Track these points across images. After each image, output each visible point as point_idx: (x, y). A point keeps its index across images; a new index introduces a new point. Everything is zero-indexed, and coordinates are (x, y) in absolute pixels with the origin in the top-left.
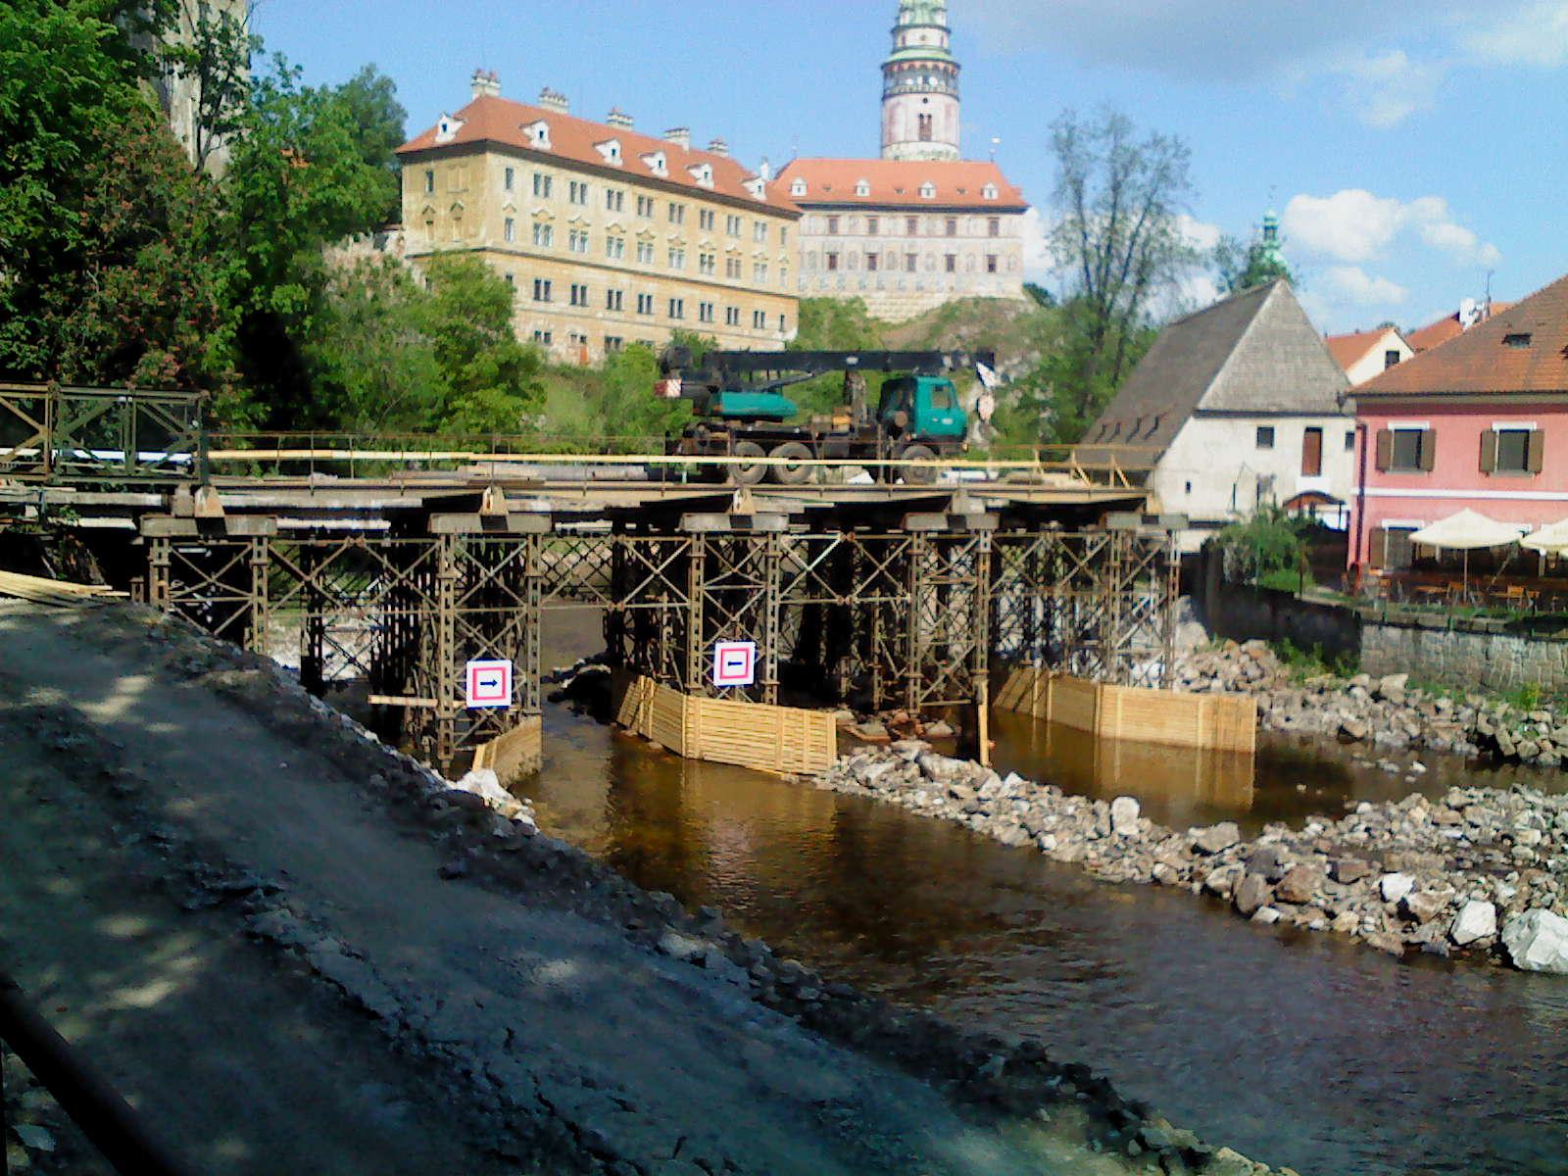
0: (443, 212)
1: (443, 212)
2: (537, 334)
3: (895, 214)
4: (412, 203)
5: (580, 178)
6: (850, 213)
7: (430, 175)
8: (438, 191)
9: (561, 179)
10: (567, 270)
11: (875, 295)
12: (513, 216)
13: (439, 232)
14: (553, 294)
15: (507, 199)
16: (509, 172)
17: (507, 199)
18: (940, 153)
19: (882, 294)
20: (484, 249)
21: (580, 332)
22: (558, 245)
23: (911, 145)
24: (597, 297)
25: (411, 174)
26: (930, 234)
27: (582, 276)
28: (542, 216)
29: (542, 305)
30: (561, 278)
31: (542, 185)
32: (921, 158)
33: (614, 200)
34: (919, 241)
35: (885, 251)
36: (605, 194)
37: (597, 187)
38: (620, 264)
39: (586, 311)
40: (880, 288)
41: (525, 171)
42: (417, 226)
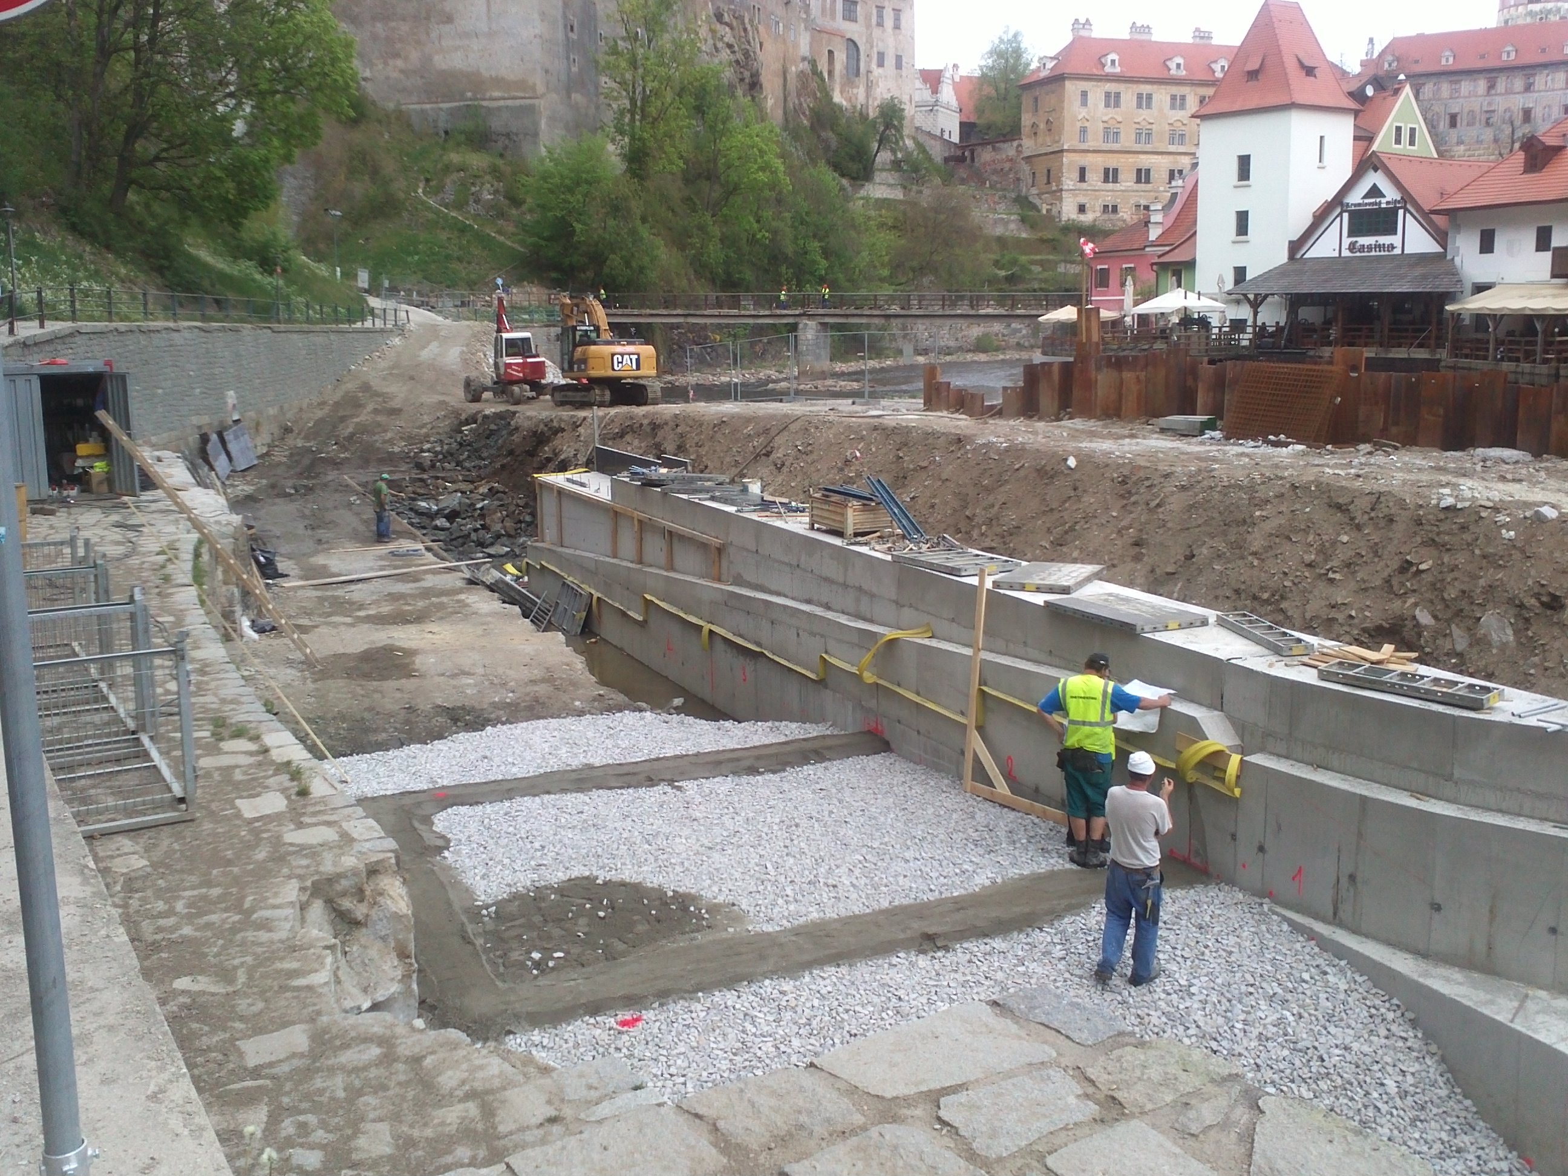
0: (1042, 126)
1: (1042, 126)
2: (1106, 207)
3: (1476, 76)
4: (1027, 119)
5: (1146, 89)
6: (1435, 80)
7: (1036, 99)
8: (1041, 112)
9: (1128, 95)
10: (1131, 159)
11: (1456, 148)
12: (1087, 124)
13: (1040, 140)
14: (1121, 177)
15: (1083, 113)
16: (1084, 94)
17: (1083, 113)
18: (1549, 11)
19: (1462, 147)
20: (1062, 151)
21: (1143, 202)
22: (1127, 140)
23: (1520, 8)
24: (1159, 176)
25: (1027, 100)
26: (1509, 92)
27: (1145, 161)
28: (1112, 122)
29: (1110, 186)
30: (1127, 165)
31: (1113, 100)
32: (1529, 20)
33: (1177, 102)
34: (1498, 99)
35: (1466, 110)
36: (1169, 98)
37: (1161, 96)
38: (1182, 149)
39: (1149, 187)
40: (1460, 142)
41: (1097, 93)
42: (1029, 137)
